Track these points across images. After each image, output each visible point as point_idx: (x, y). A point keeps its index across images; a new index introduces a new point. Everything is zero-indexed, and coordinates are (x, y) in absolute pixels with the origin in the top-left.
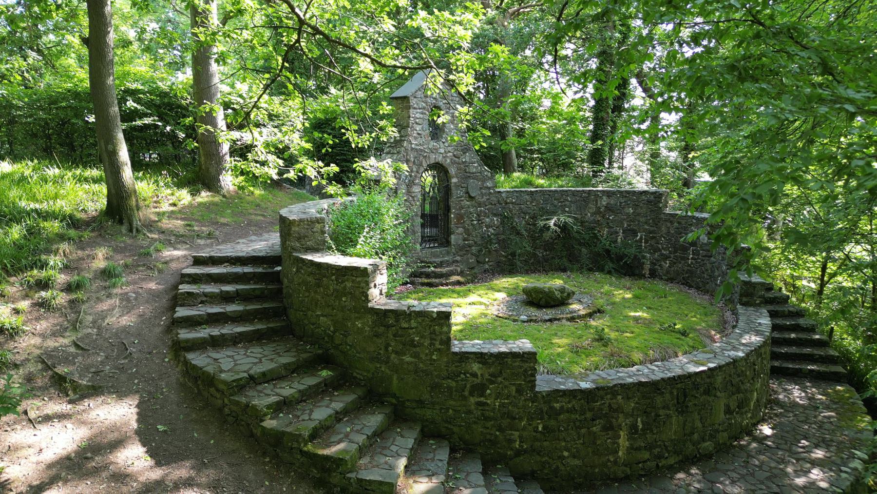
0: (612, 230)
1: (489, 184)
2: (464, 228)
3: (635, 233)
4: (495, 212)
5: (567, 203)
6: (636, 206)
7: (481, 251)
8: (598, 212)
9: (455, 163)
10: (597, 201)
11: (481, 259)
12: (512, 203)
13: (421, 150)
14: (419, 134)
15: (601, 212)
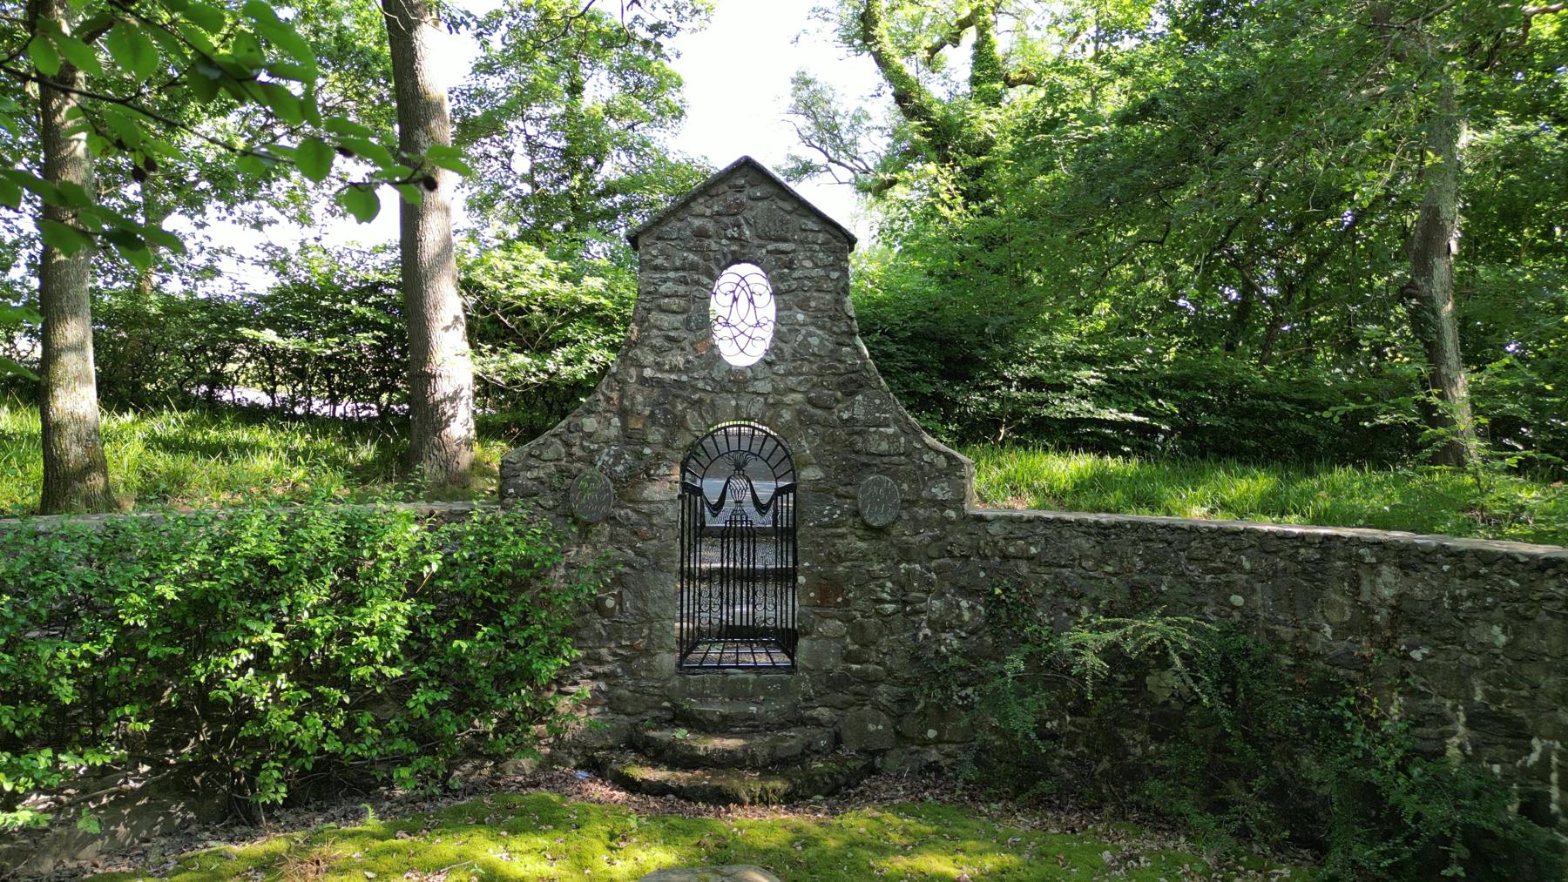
0: (1421, 706)
1: (940, 491)
2: (848, 620)
3: (1519, 736)
4: (963, 581)
5: (1236, 576)
6: (1518, 622)
7: (906, 701)
8: (1361, 623)
9: (812, 421)
10: (1356, 582)
11: (909, 725)
12: (1031, 559)
13: (678, 384)
14: (669, 339)
15: (1374, 628)
